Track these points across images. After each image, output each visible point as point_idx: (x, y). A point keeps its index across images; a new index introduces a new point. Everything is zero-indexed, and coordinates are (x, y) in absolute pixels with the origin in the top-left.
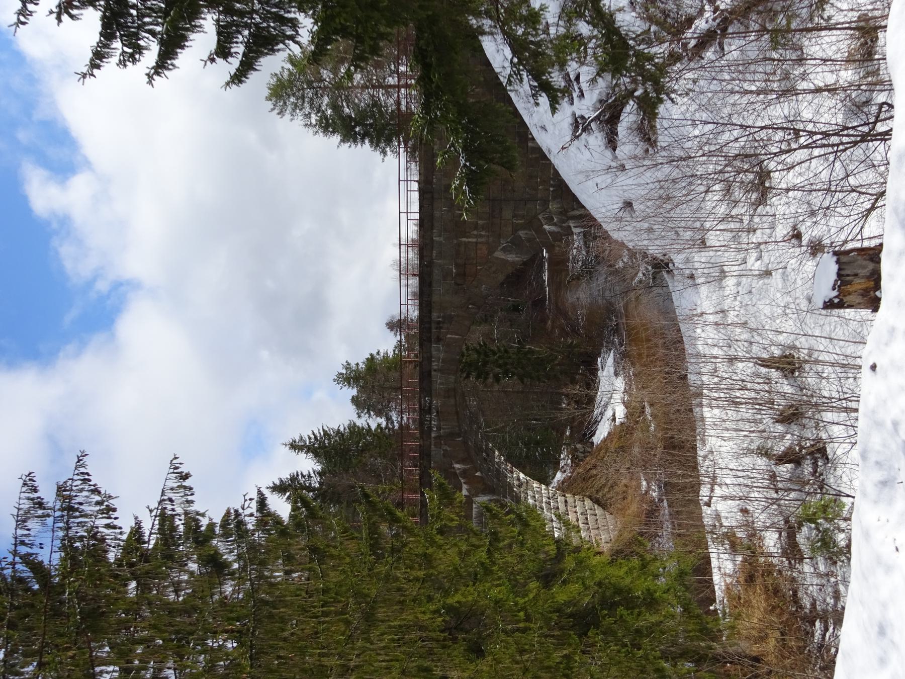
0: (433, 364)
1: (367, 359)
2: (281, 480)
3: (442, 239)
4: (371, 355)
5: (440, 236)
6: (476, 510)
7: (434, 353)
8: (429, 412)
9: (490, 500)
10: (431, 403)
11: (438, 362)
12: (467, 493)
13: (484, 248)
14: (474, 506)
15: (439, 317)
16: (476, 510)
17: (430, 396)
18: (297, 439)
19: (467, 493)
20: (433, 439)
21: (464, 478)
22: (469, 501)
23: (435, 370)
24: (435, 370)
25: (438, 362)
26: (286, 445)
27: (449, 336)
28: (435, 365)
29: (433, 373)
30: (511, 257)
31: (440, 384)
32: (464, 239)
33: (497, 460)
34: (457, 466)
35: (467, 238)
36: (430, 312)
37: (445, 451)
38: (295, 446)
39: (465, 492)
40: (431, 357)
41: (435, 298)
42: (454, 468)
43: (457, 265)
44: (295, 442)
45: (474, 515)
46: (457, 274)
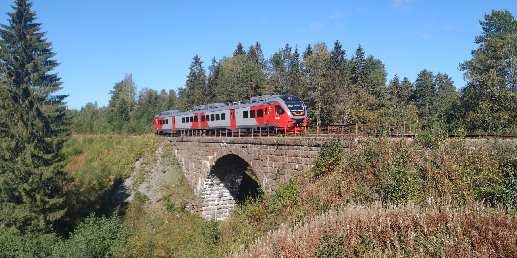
1: (447, 77)
2: (340, 47)
3: (269, 149)
4: (450, 79)
5: (270, 149)
8: (227, 143)
13: (266, 170)
14: (207, 161)
17: (230, 143)
18: (363, 51)
22: (208, 159)
26: (360, 46)
28: (237, 145)
29: (235, 144)
30: (264, 183)
32: (269, 160)
33: (238, 169)
34: (215, 155)
35: (269, 162)
36: (250, 144)
38: (360, 50)
39: (210, 157)
40: (239, 143)
43: (262, 156)
44: (361, 50)
46: (259, 157)
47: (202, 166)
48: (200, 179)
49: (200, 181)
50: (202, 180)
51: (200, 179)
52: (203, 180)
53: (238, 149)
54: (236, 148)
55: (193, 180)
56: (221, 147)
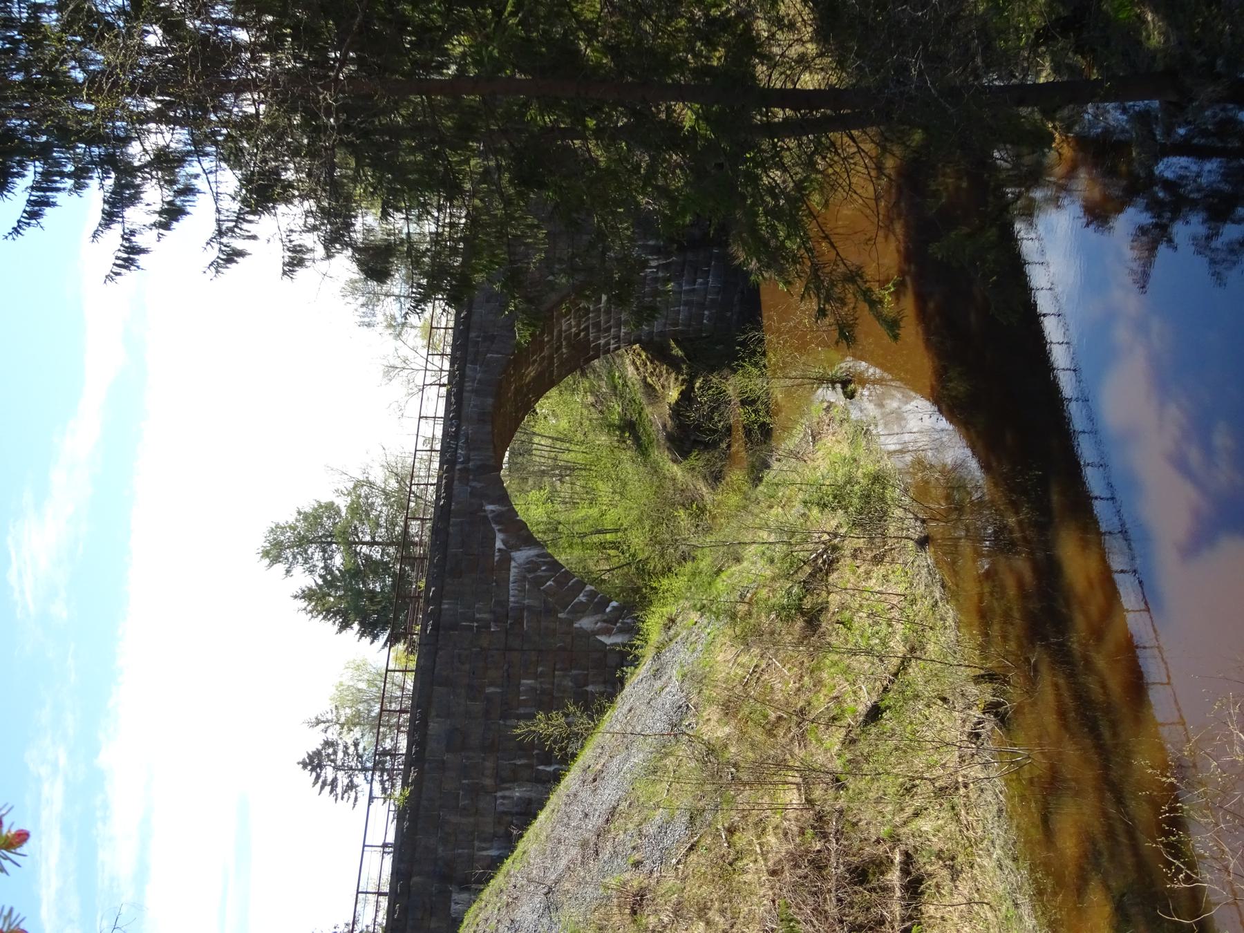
0: (467, 384)
6: (516, 570)
7: (468, 372)
9: (538, 556)
10: (458, 427)
11: (473, 381)
12: (502, 547)
14: (513, 564)
15: (478, 337)
16: (516, 570)
19: (502, 547)
20: (457, 472)
21: (497, 523)
22: (506, 559)
23: (468, 392)
24: (468, 392)
25: (473, 381)
27: (489, 355)
28: (468, 385)
29: (465, 394)
31: (475, 406)
34: (490, 507)
37: (473, 488)
39: (499, 544)
41: (475, 318)
42: (485, 511)
45: (511, 579)
47: (529, 608)
48: (576, 625)
49: (586, 623)
50: (580, 611)
51: (576, 625)
52: (582, 598)
53: (480, 382)
54: (475, 392)
55: (590, 688)
56: (465, 470)
